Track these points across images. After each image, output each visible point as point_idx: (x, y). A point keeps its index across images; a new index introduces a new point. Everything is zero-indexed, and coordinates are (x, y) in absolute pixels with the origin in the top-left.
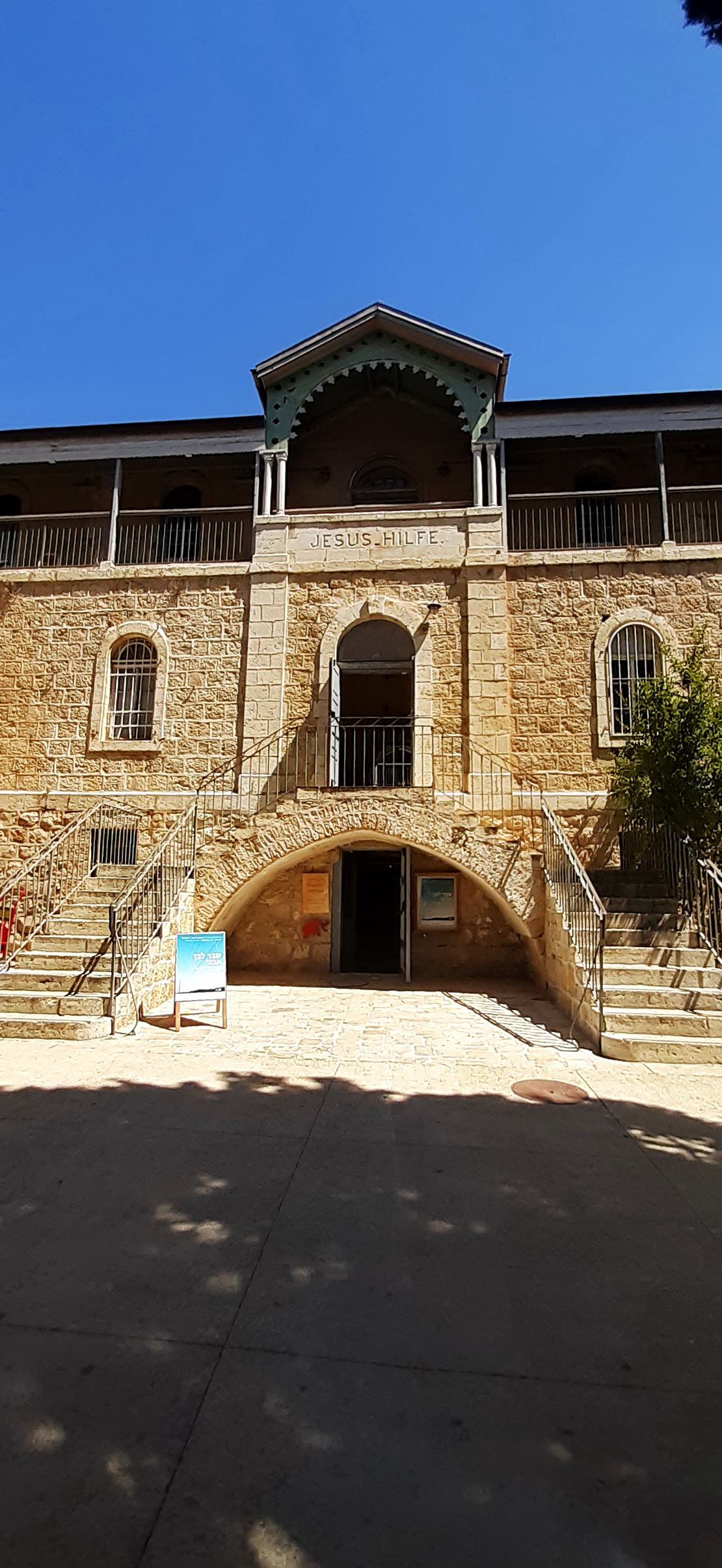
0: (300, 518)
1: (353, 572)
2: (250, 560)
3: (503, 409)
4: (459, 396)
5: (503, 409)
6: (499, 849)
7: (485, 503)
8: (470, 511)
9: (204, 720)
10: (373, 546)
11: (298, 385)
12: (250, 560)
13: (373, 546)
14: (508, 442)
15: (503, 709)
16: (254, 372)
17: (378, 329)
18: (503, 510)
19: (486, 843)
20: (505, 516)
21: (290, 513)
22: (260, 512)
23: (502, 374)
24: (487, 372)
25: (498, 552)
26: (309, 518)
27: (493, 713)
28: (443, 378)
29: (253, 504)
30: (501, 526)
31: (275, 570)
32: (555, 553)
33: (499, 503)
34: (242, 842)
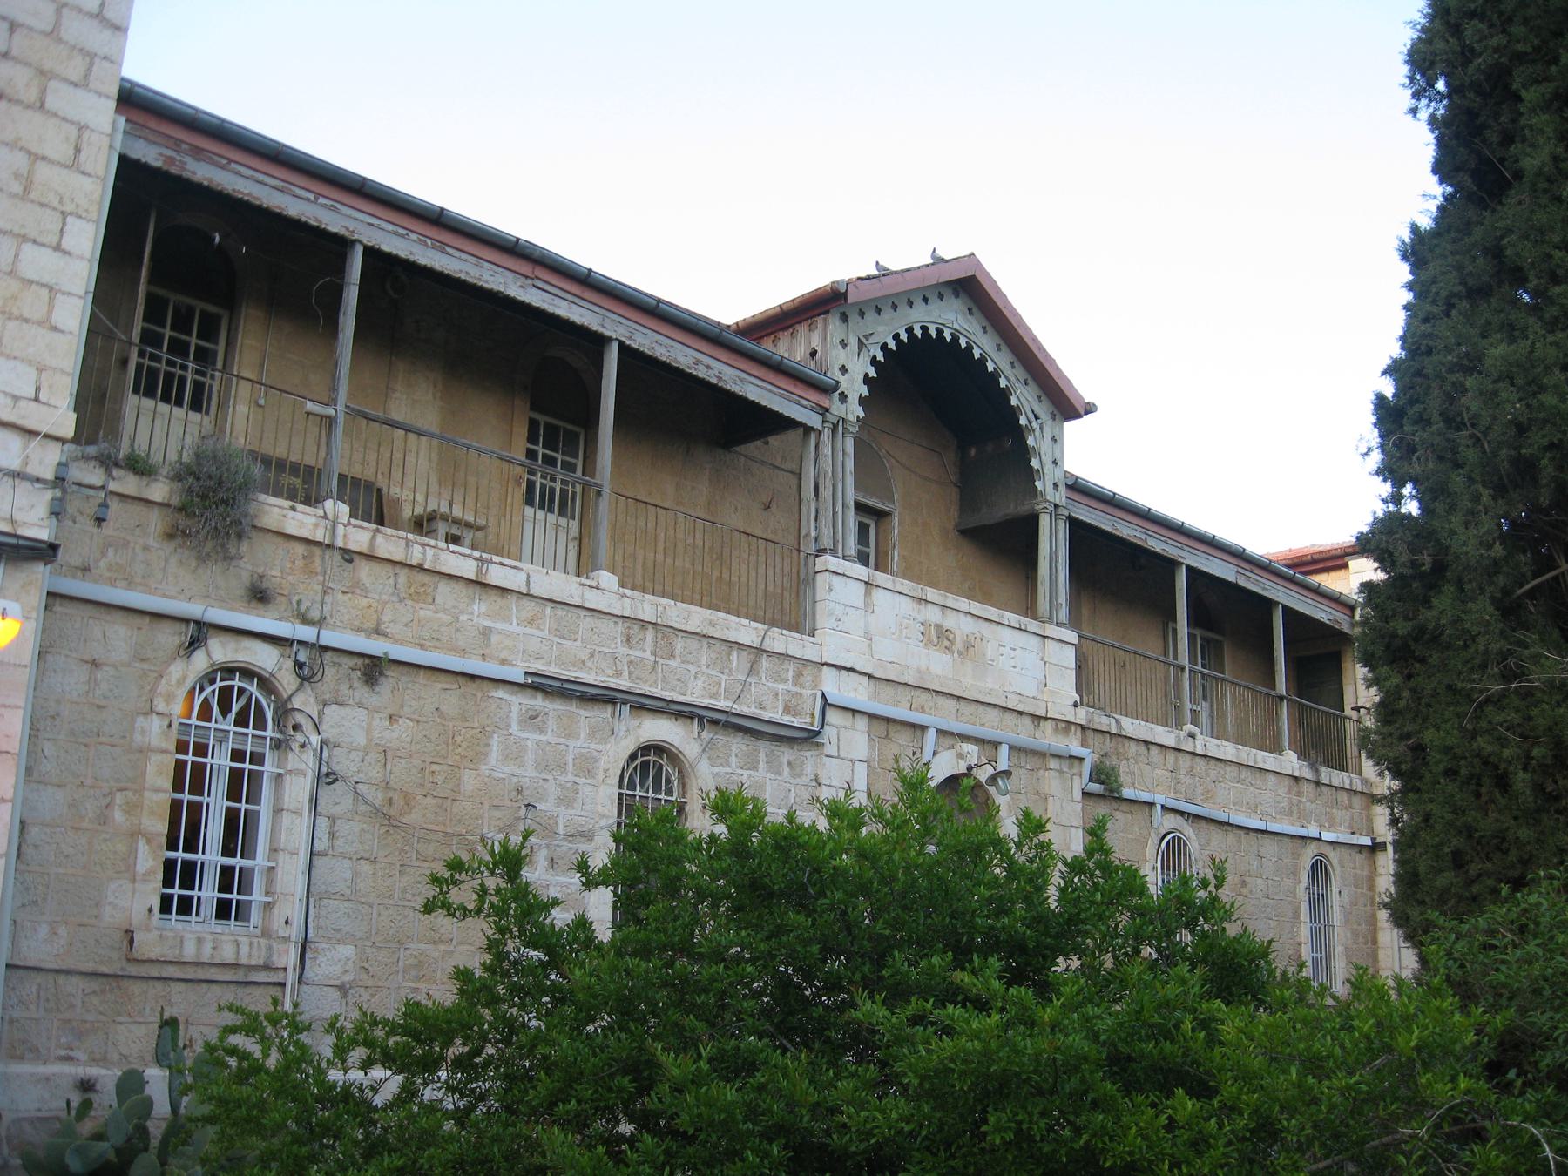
31: (857, 668)
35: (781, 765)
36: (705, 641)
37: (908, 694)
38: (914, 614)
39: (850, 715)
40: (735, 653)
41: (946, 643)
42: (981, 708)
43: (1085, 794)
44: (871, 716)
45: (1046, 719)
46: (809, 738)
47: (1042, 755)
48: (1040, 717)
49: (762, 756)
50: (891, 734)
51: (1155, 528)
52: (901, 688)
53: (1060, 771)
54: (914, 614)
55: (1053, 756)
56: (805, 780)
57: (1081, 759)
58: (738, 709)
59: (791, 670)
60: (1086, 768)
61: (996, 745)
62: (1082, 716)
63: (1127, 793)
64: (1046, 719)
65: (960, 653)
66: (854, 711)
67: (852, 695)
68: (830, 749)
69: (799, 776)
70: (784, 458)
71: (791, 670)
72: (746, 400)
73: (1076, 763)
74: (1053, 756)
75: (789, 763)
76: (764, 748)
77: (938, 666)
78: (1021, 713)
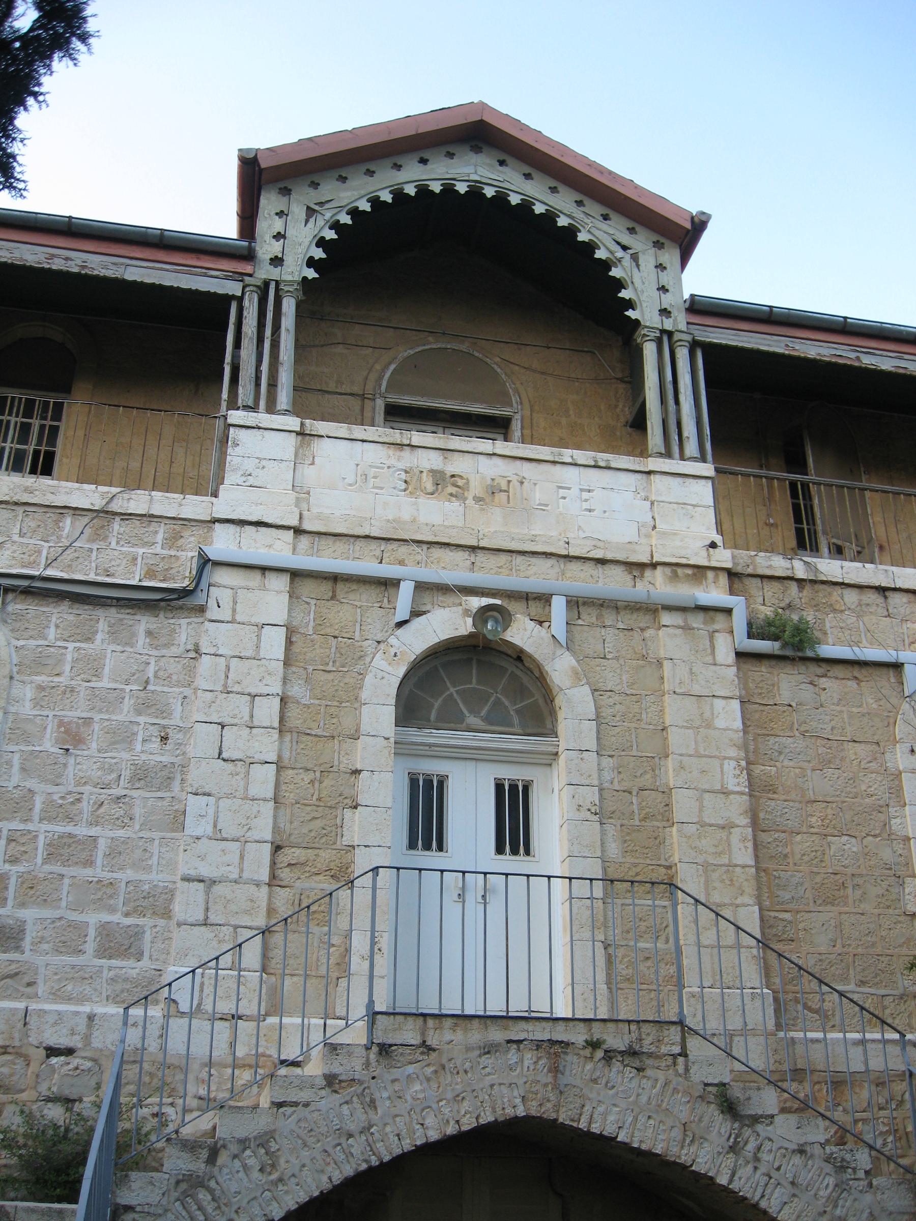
0: (322, 427)
1: (431, 544)
6: (828, 1168)
8: (654, 464)
9: (82, 831)
10: (470, 502)
13: (470, 502)
15: (744, 855)
19: (801, 1151)
25: (713, 545)
27: (725, 860)
34: (234, 1148)
35: (133, 635)
36: (20, 510)
37: (375, 548)
38: (392, 461)
39: (257, 575)
40: (68, 521)
41: (453, 490)
42: (520, 559)
43: (741, 656)
44: (296, 575)
45: (654, 566)
46: (178, 600)
47: (651, 610)
48: (642, 566)
49: (102, 625)
50: (340, 595)
51: (873, 344)
52: (360, 543)
53: (687, 628)
54: (392, 461)
55: (669, 608)
56: (174, 650)
57: (728, 611)
58: (51, 572)
59: (161, 532)
60: (739, 621)
61: (545, 599)
62: (724, 557)
63: (828, 650)
64: (654, 566)
65: (478, 499)
66: (264, 569)
67: (263, 551)
68: (213, 612)
69: (167, 645)
70: (339, 382)
71: (161, 532)
72: (124, 281)
73: (720, 617)
74: (669, 608)
75: (149, 633)
76: (104, 619)
77: (436, 515)
78: (602, 562)
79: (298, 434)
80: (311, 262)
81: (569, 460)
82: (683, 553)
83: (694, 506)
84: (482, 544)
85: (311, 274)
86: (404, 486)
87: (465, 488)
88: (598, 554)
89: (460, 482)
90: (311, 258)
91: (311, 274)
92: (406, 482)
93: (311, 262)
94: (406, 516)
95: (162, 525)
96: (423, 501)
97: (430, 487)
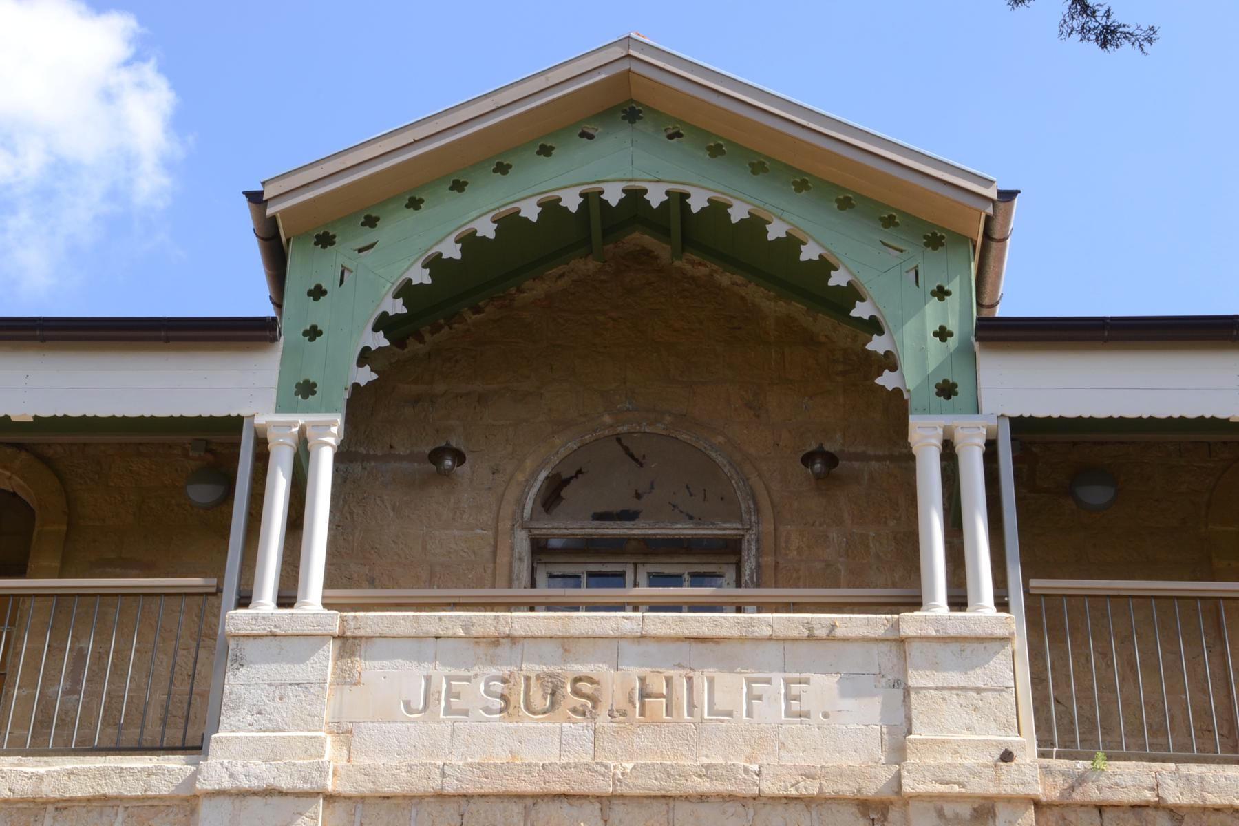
0: (373, 621)
2: (195, 747)
3: (1002, 333)
4: (867, 282)
5: (1002, 333)
7: (958, 601)
8: (910, 622)
11: (383, 234)
12: (195, 747)
13: (603, 719)
14: (1020, 425)
16: (255, 198)
17: (625, 98)
18: (1014, 623)
20: (1021, 643)
21: (340, 607)
22: (244, 601)
23: (991, 238)
24: (956, 227)
25: (1007, 756)
26: (402, 621)
28: (821, 236)
29: (219, 572)
30: (1011, 670)
31: (284, 784)
32: (1195, 769)
33: (1002, 604)
79: (341, 637)
80: (366, 357)
81: (767, 631)
82: (955, 777)
83: (978, 690)
84: (621, 789)
85: (365, 375)
86: (499, 704)
87: (595, 701)
88: (810, 788)
89: (586, 687)
90: (366, 350)
91: (365, 375)
92: (503, 697)
93: (366, 357)
94: (502, 757)
95: (121, 810)
96: (530, 724)
97: (540, 700)
